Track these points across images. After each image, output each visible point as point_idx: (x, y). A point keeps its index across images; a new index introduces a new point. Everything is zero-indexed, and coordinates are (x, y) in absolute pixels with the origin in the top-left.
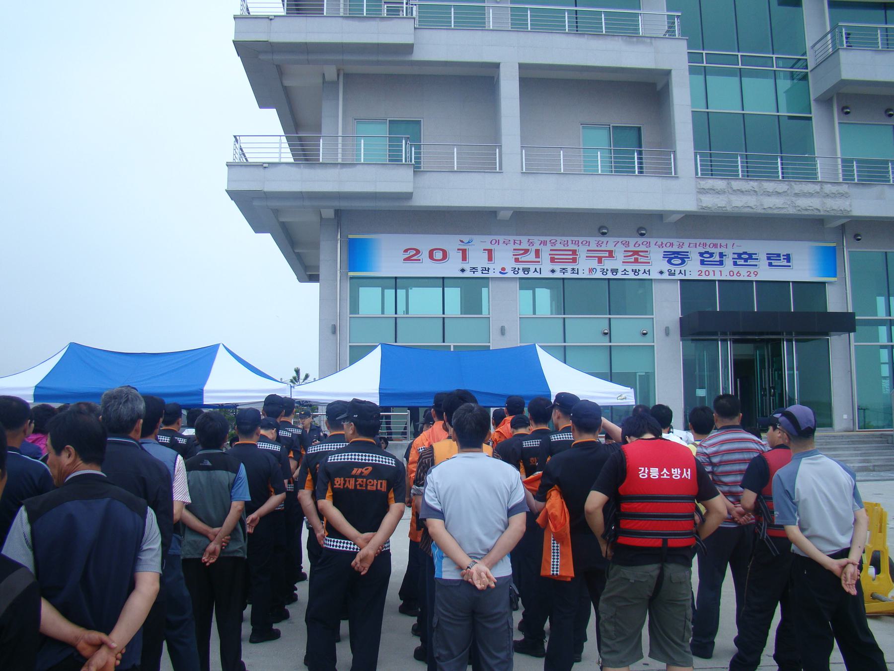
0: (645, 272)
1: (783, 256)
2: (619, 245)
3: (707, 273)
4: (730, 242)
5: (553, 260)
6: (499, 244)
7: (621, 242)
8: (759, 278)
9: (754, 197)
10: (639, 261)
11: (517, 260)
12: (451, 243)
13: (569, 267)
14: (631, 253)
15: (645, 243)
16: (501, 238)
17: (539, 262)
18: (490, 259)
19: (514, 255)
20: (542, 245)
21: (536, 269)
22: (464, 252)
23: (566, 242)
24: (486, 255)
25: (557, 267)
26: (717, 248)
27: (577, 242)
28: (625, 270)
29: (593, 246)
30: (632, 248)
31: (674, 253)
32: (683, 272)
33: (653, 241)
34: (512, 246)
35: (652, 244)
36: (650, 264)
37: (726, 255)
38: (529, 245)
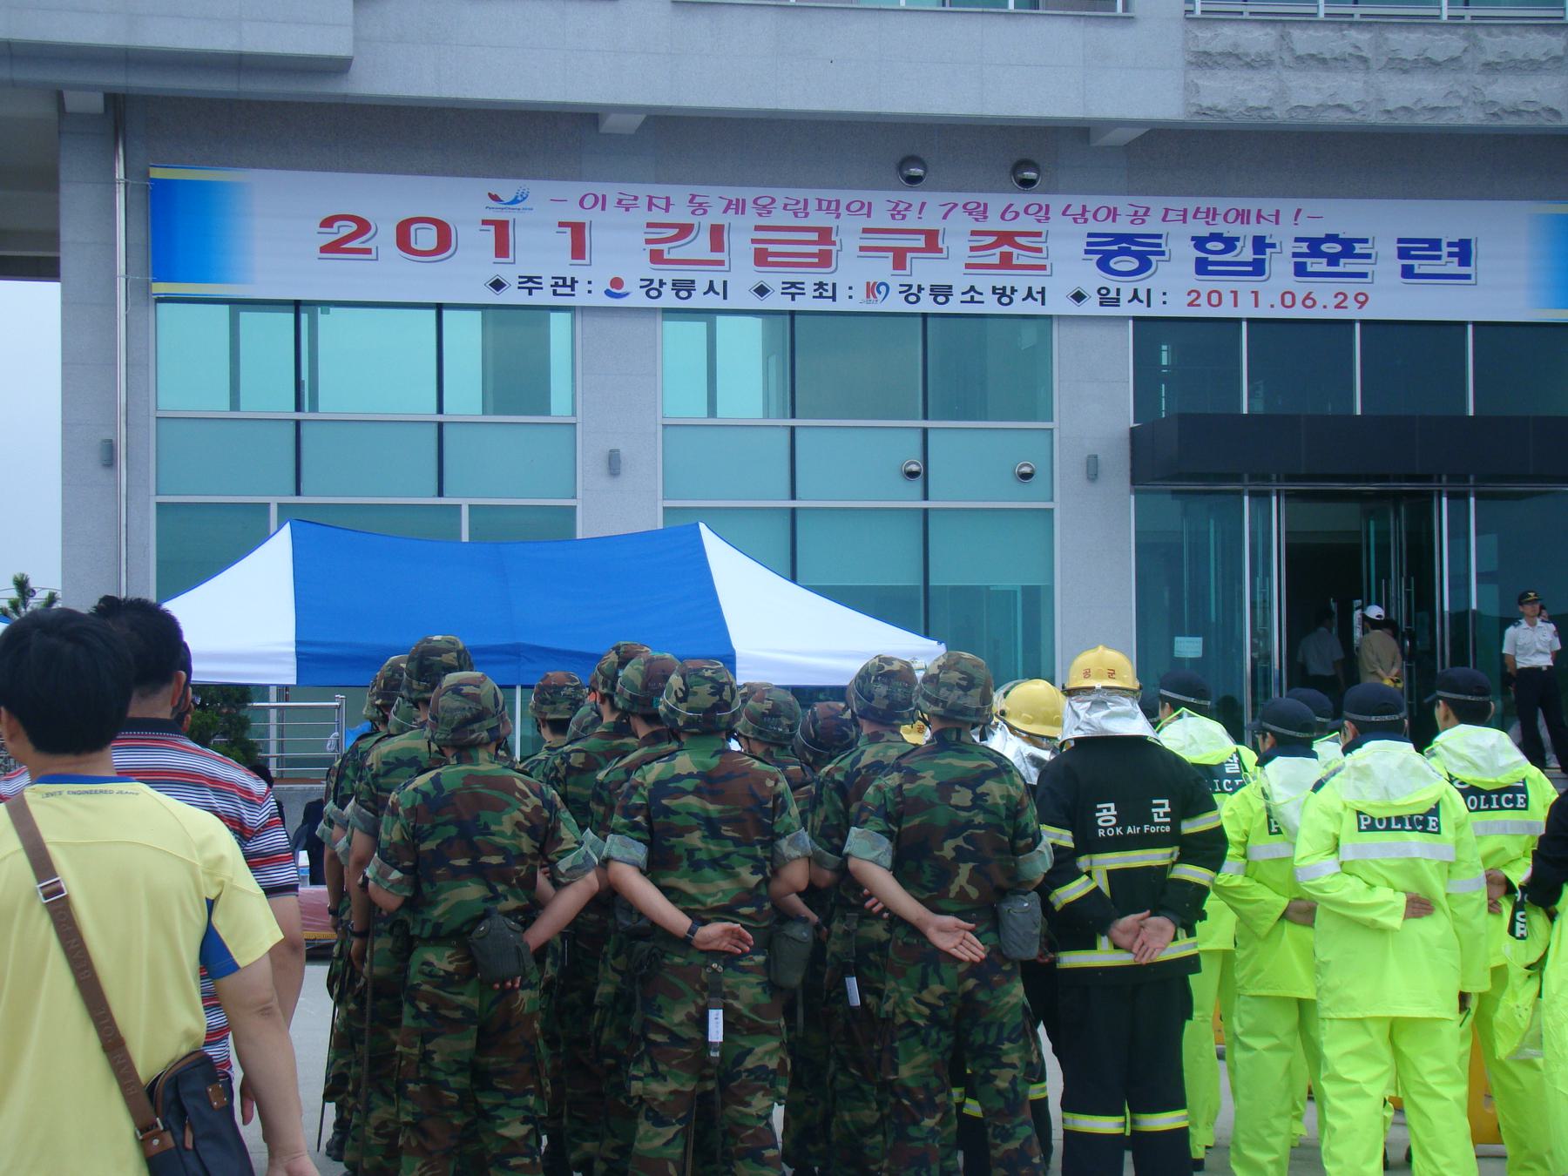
0: (1030, 294)
1: (1450, 245)
2: (960, 208)
3: (1215, 297)
4: (1287, 206)
5: (761, 258)
6: (603, 208)
7: (965, 207)
8: (1369, 313)
9: (1360, 76)
10: (1015, 262)
11: (656, 257)
13: (809, 278)
14: (990, 240)
15: (1033, 209)
16: (612, 191)
17: (721, 263)
18: (578, 251)
19: (648, 242)
20: (731, 212)
21: (711, 282)
22: (501, 228)
23: (801, 205)
24: (566, 237)
25: (774, 279)
26: (1248, 223)
27: (833, 206)
28: (972, 288)
29: (881, 219)
30: (994, 223)
31: (1119, 238)
32: (1143, 296)
33: (1057, 202)
34: (641, 215)
35: (1055, 212)
36: (1048, 272)
37: (1273, 246)
38: (693, 213)
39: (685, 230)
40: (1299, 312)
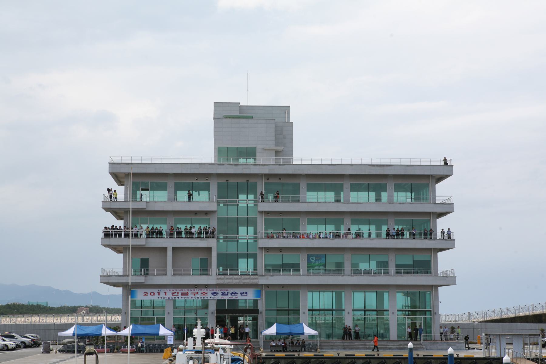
2: (200, 291)
4: (230, 289)
5: (182, 295)
11: (173, 295)
12: (156, 291)
13: (186, 296)
16: (169, 289)
18: (166, 295)
22: (159, 293)
25: (183, 297)
29: (193, 291)
30: (203, 291)
31: (214, 292)
33: (209, 289)
34: (171, 291)
35: (209, 290)
39: (175, 293)
40: (231, 299)
